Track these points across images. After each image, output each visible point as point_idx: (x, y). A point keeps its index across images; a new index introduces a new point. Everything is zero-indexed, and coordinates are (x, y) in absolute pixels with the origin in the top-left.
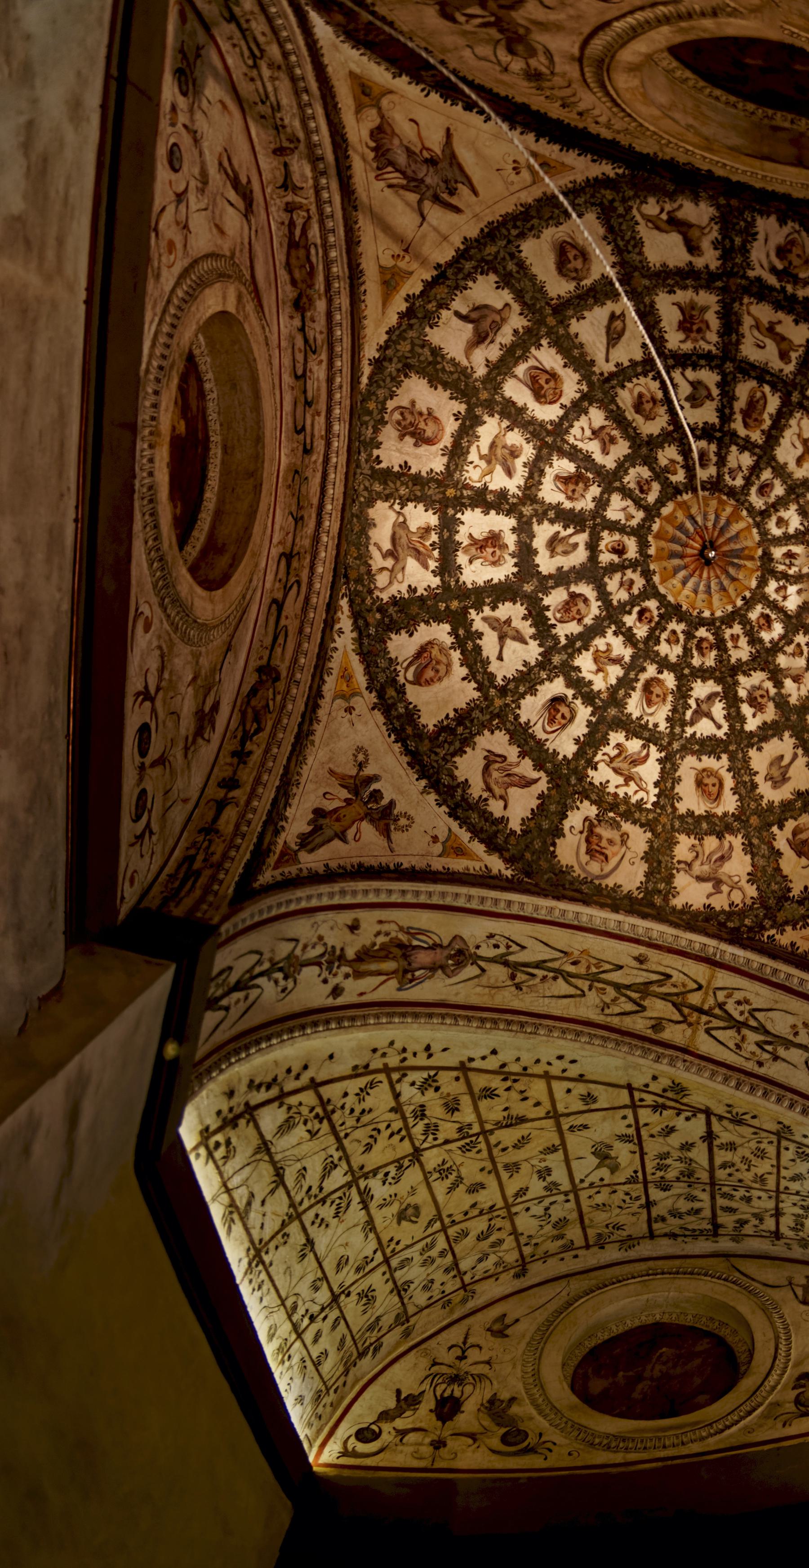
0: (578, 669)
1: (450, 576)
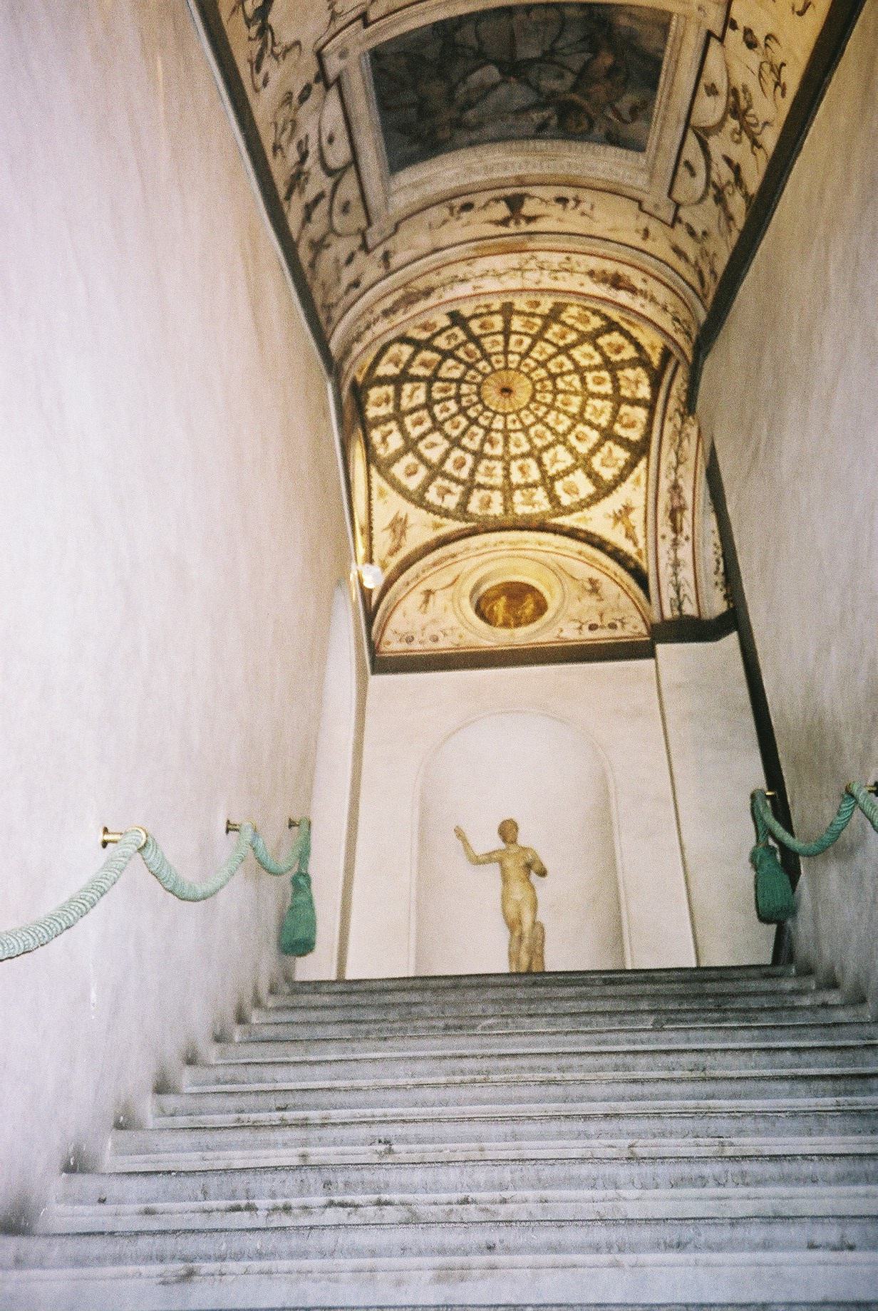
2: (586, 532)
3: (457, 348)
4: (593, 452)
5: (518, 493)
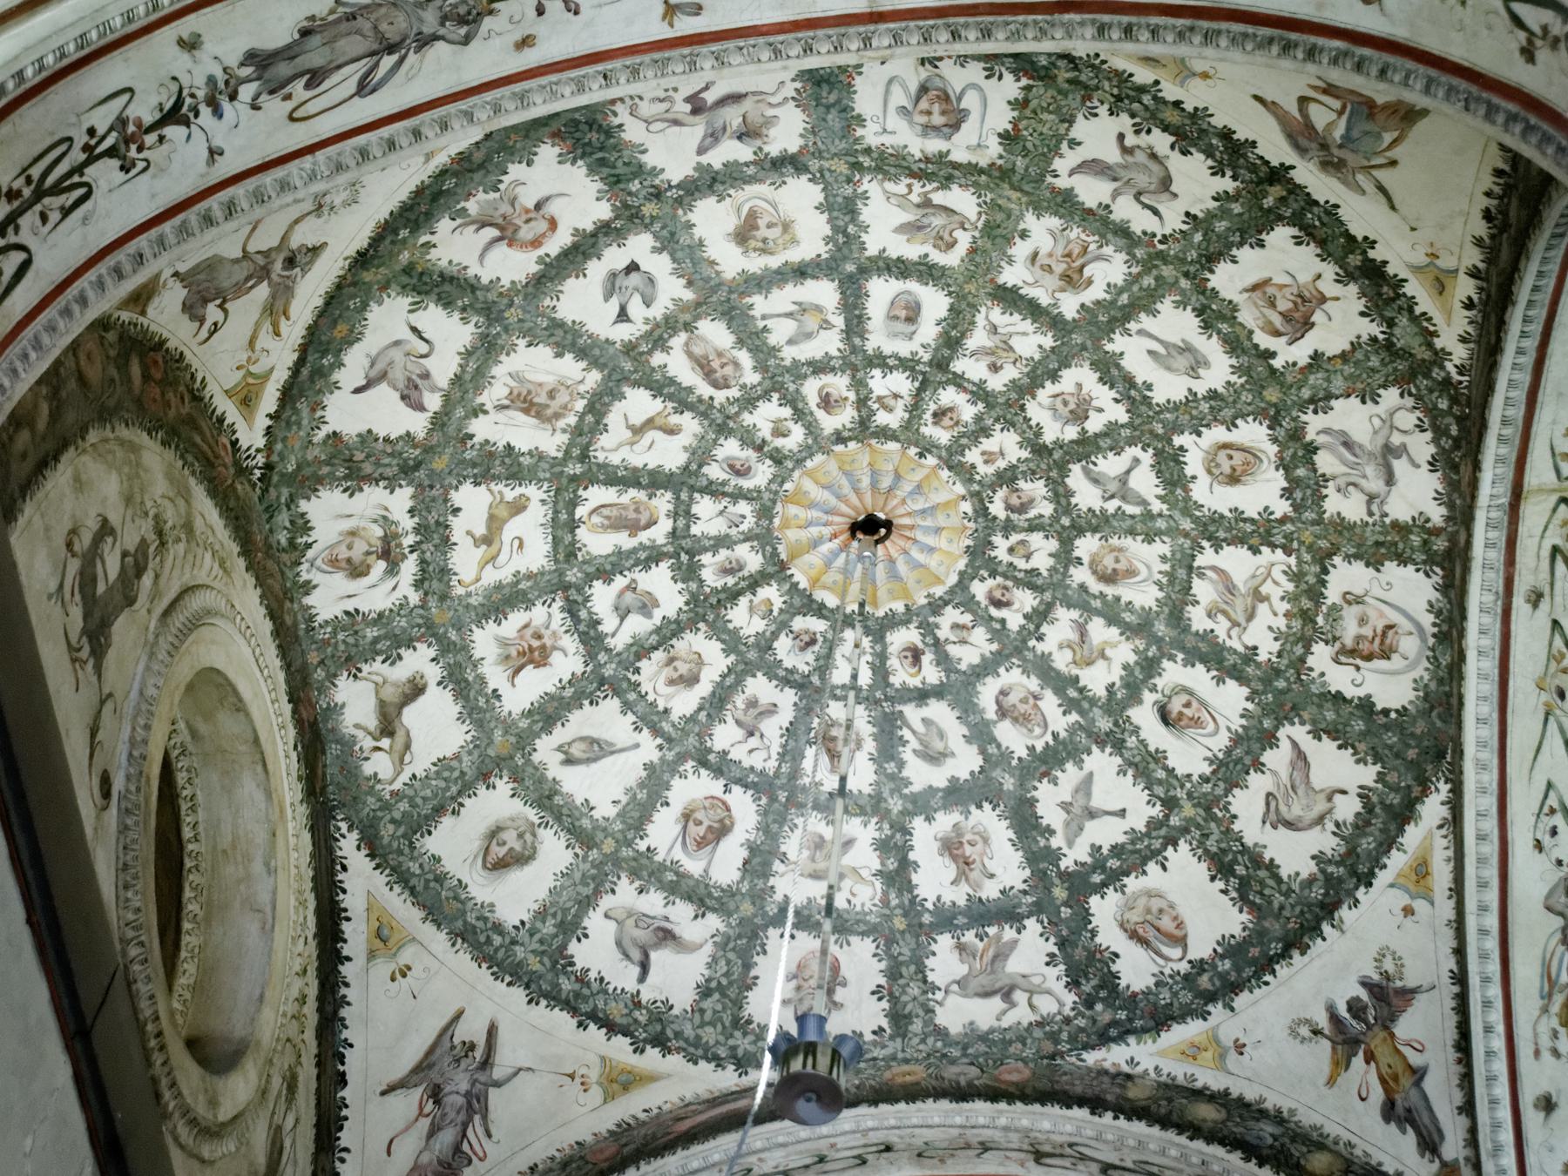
0: (1110, 688)
1: (1019, 905)
2: (1220, 1098)
3: (658, 336)
4: (1234, 766)
5: (944, 942)
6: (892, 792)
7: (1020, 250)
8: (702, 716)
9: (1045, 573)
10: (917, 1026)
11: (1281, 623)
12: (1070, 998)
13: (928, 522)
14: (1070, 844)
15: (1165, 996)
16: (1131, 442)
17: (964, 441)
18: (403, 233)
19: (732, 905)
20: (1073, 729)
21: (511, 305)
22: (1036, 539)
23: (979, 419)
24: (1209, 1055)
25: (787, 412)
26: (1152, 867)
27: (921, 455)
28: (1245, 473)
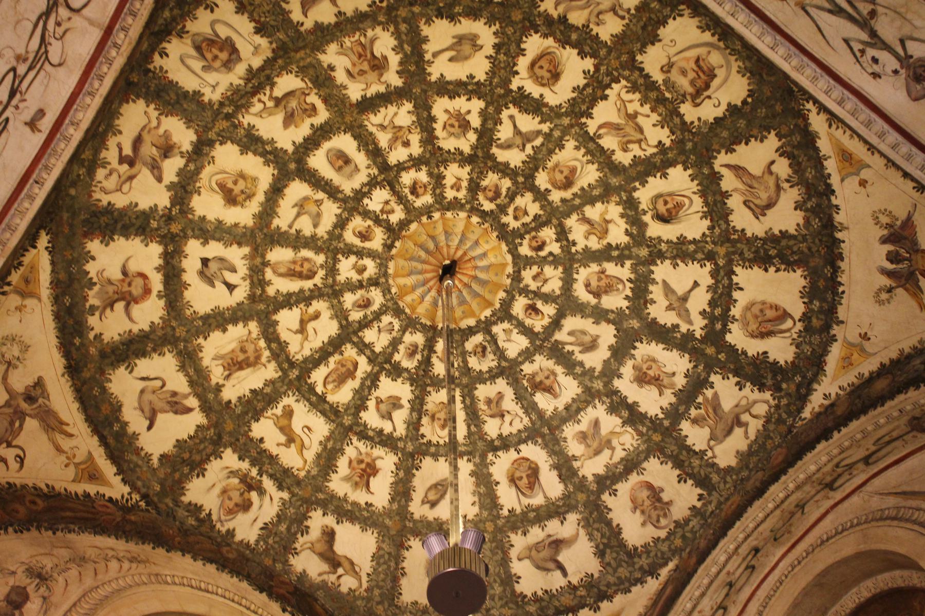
0: (627, 233)
2: (883, 371)
4: (717, 208)
6: (591, 380)
7: (340, 77)
8: (473, 428)
9: (541, 212)
10: (715, 478)
11: (655, 117)
12: (767, 395)
13: (469, 244)
14: (690, 322)
15: (807, 349)
16: (499, 111)
17: (438, 191)
18: (77, 341)
19: (573, 502)
20: (634, 269)
21: (174, 329)
22: (520, 201)
23: (430, 174)
24: (855, 356)
25: (353, 259)
26: (736, 295)
27: (430, 217)
28: (556, 67)
